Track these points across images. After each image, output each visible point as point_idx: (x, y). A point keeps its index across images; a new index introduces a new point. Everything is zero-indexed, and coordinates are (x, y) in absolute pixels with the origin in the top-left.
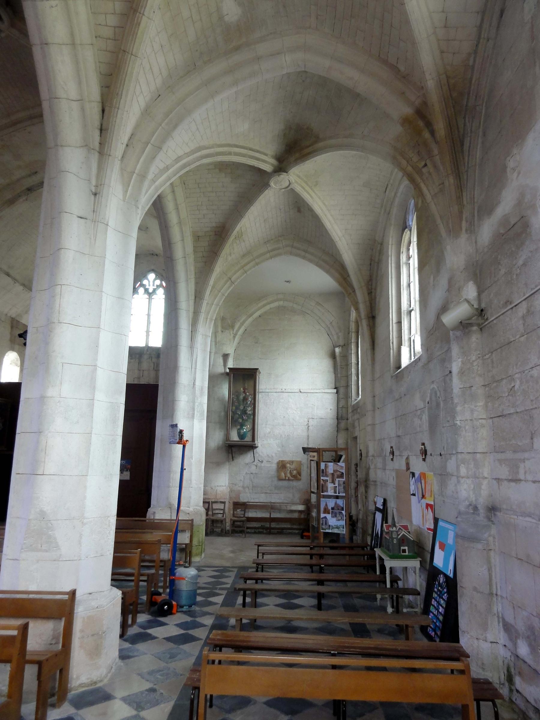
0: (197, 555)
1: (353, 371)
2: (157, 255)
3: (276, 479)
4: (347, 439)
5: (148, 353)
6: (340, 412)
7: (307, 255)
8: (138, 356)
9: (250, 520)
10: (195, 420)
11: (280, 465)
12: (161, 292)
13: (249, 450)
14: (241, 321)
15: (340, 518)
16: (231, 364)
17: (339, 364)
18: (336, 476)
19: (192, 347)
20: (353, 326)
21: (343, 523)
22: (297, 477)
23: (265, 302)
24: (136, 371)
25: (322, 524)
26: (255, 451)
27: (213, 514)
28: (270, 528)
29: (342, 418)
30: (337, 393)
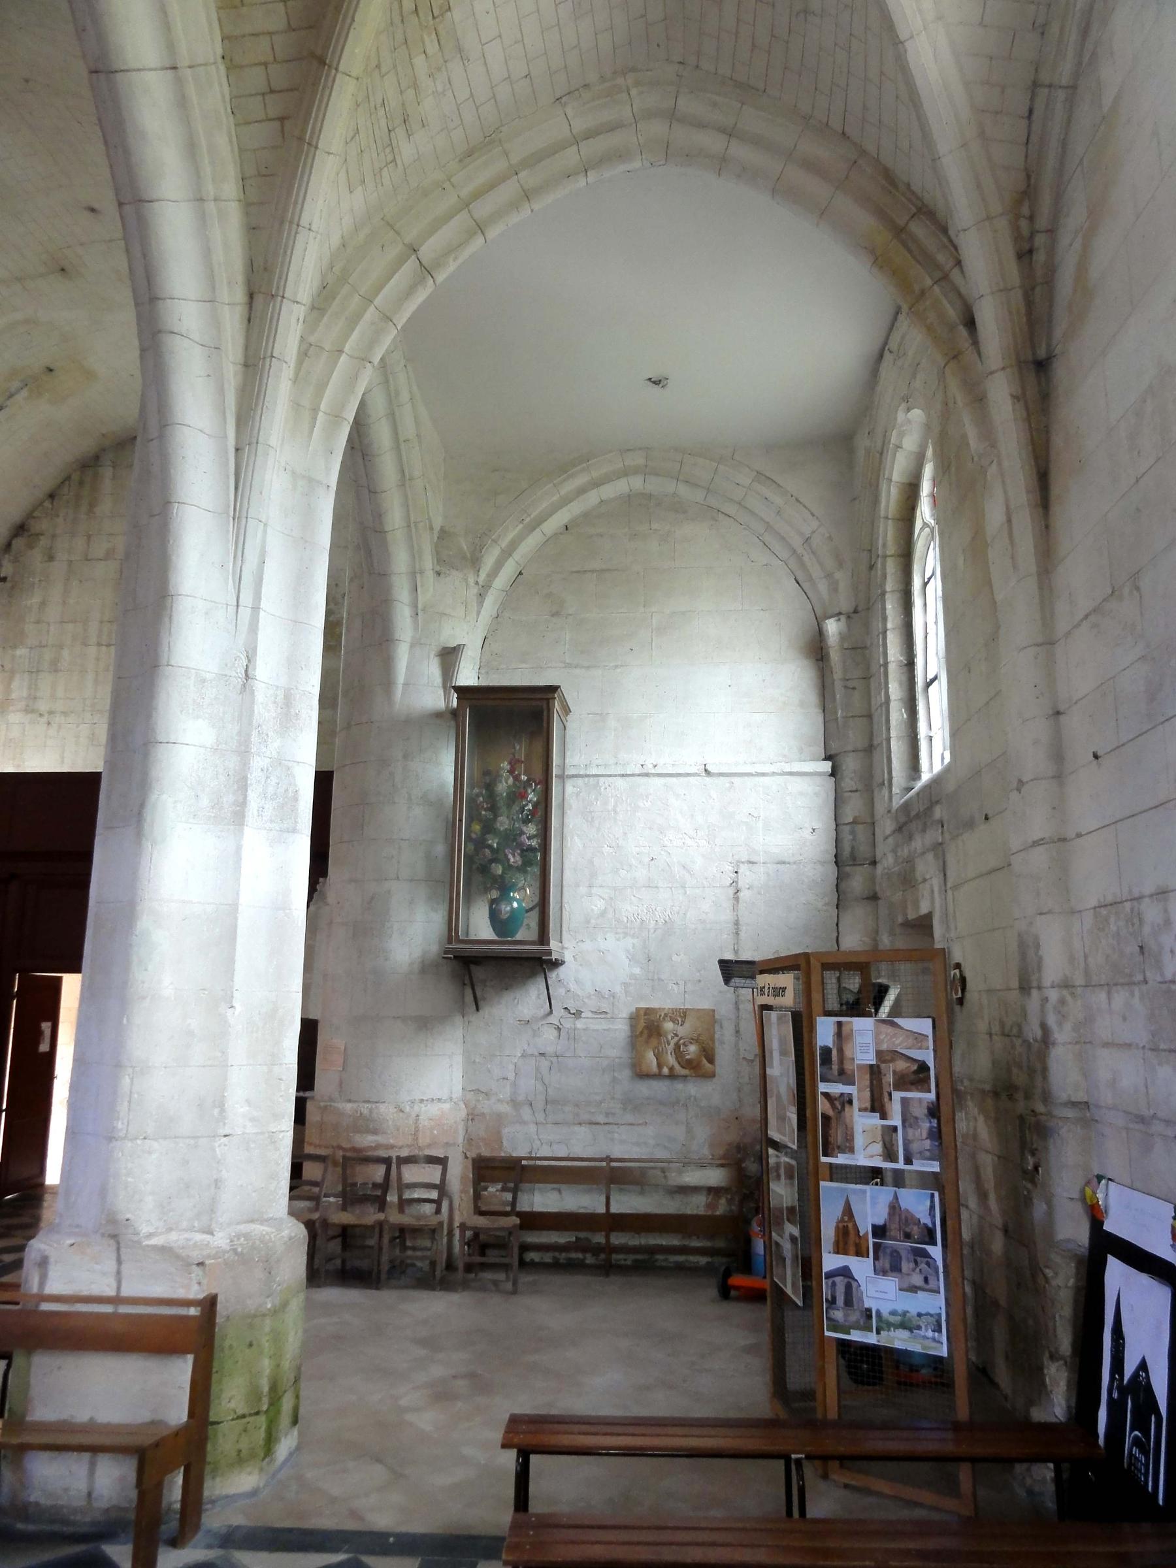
0: (240, 1460)
1: (895, 690)
3: (627, 1073)
4: (877, 932)
6: (847, 838)
7: (740, 151)
9: (532, 1221)
10: (247, 830)
11: (642, 1024)
13: (532, 975)
14: (504, 543)
15: (917, 1280)
16: (467, 676)
17: (838, 674)
18: (889, 1078)
19: (238, 510)
20: (888, 535)
21: (934, 1303)
22: (699, 1065)
23: (581, 480)
25: (832, 1302)
26: (553, 976)
27: (403, 1204)
28: (611, 1249)
29: (854, 860)
30: (833, 774)
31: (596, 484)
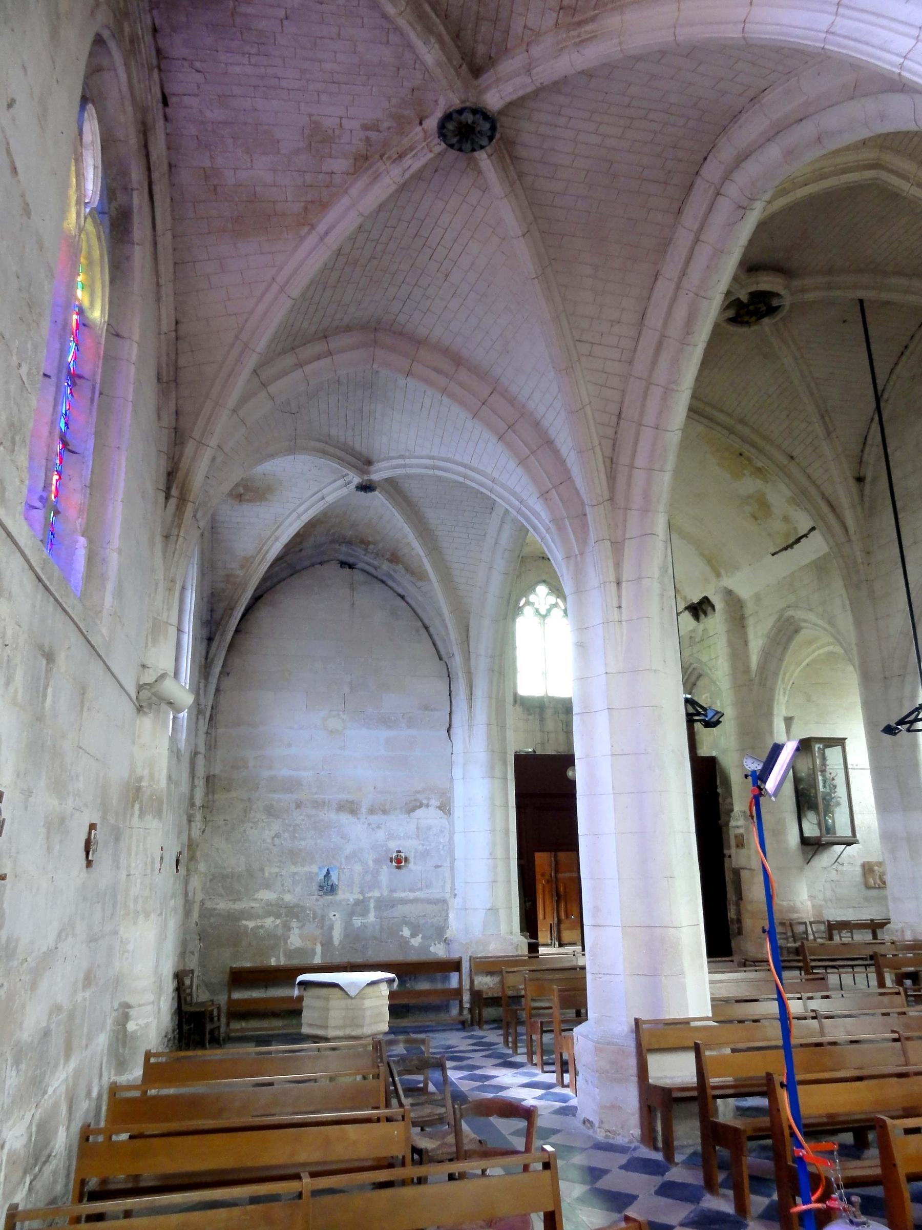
3: (863, 887)
5: (552, 705)
8: (538, 710)
12: (557, 613)
24: (539, 734)
31: (819, 648)
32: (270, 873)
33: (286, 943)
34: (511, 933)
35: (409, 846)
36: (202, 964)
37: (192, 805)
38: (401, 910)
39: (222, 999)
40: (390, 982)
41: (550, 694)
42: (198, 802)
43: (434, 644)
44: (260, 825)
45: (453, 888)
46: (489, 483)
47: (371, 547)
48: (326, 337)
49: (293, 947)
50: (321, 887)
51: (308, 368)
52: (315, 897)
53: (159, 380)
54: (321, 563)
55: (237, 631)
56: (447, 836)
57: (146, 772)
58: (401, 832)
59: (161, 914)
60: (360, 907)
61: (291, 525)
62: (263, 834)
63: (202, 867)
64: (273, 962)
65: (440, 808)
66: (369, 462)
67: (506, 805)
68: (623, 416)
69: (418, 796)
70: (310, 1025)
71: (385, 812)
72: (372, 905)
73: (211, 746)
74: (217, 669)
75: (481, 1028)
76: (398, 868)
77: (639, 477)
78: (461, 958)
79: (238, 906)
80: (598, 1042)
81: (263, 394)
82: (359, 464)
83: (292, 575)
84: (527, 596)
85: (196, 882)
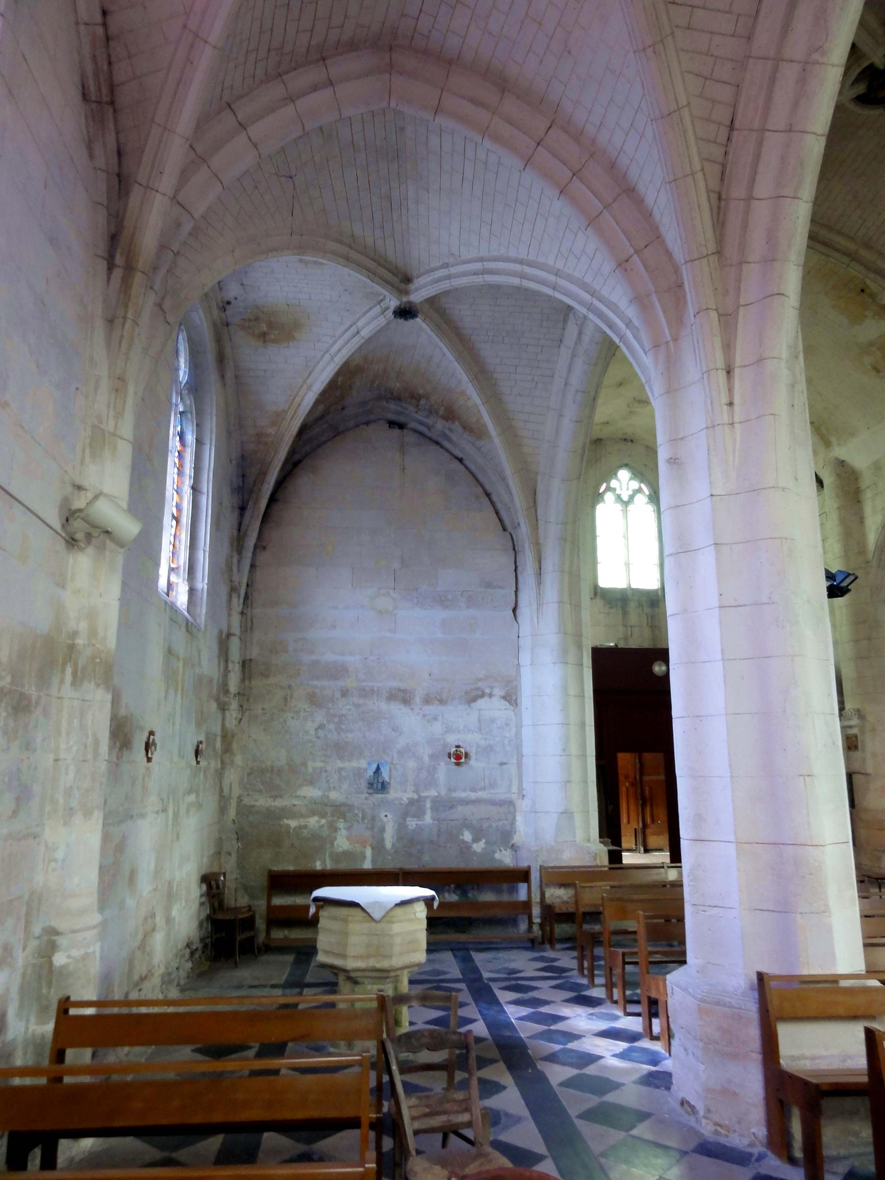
2: (632, 441)
8: (620, 604)
12: (641, 500)
24: (621, 629)
32: (314, 769)
33: (332, 845)
34: (589, 840)
35: (470, 740)
36: (240, 866)
37: (224, 688)
38: (461, 811)
39: (261, 905)
40: (428, 901)
41: (634, 586)
42: (233, 688)
43: (497, 513)
44: (302, 714)
45: (521, 788)
46: (552, 278)
47: (422, 402)
48: (324, 59)
49: (340, 850)
50: (371, 785)
51: (303, 103)
52: (364, 796)
53: (85, 96)
54: (367, 423)
55: (273, 499)
56: (514, 730)
57: (83, 626)
58: (460, 724)
59: (164, 810)
60: (415, 807)
61: (324, 369)
62: (306, 725)
63: (238, 760)
64: (318, 866)
65: (504, 698)
66: (408, 280)
67: (582, 696)
68: (737, 124)
69: (480, 684)
70: (326, 952)
71: (442, 702)
72: (428, 805)
73: (248, 627)
74: (251, 542)
75: (552, 948)
76: (458, 764)
77: (761, 211)
78: (529, 867)
79: (279, 803)
80: (702, 1001)
81: (241, 140)
82: (395, 280)
83: (335, 437)
84: (608, 482)
85: (232, 777)
